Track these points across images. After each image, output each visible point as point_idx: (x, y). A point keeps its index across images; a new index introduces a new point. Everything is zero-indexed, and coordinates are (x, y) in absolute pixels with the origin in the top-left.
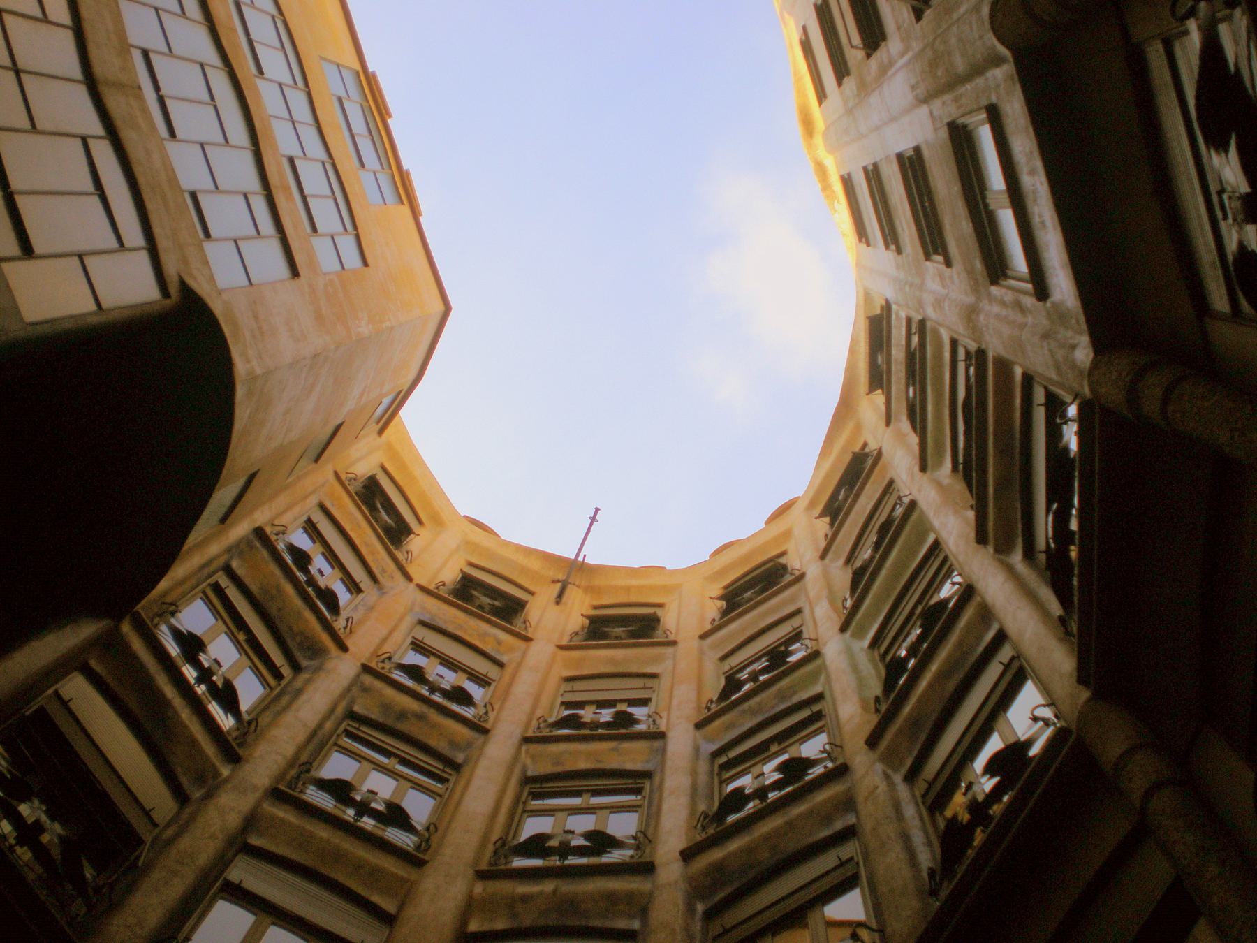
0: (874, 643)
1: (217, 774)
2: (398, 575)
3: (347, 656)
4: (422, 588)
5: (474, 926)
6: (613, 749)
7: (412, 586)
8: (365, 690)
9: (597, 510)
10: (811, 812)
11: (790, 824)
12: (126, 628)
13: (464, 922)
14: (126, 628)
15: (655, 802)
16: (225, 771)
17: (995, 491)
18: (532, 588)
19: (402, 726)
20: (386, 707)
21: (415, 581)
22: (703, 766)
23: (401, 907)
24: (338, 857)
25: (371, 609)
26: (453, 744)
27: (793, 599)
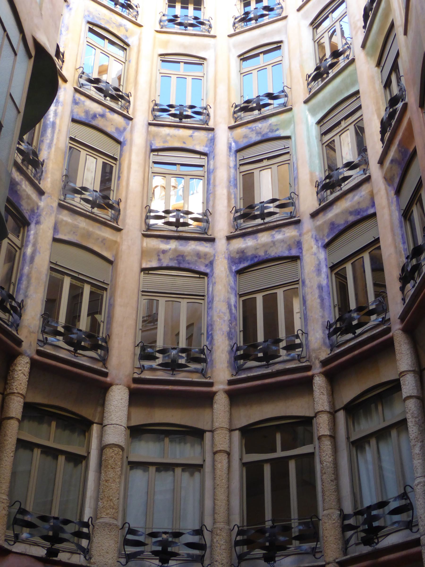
0: (318, 123)
5: (144, 266)
6: (191, 136)
10: (283, 241)
11: (274, 243)
13: (141, 264)
15: (212, 181)
16: (42, 204)
17: (392, 161)
19: (94, 123)
20: (87, 112)
22: (232, 164)
23: (116, 256)
24: (88, 235)
25: (68, 29)
26: (117, 129)
27: (279, 31)
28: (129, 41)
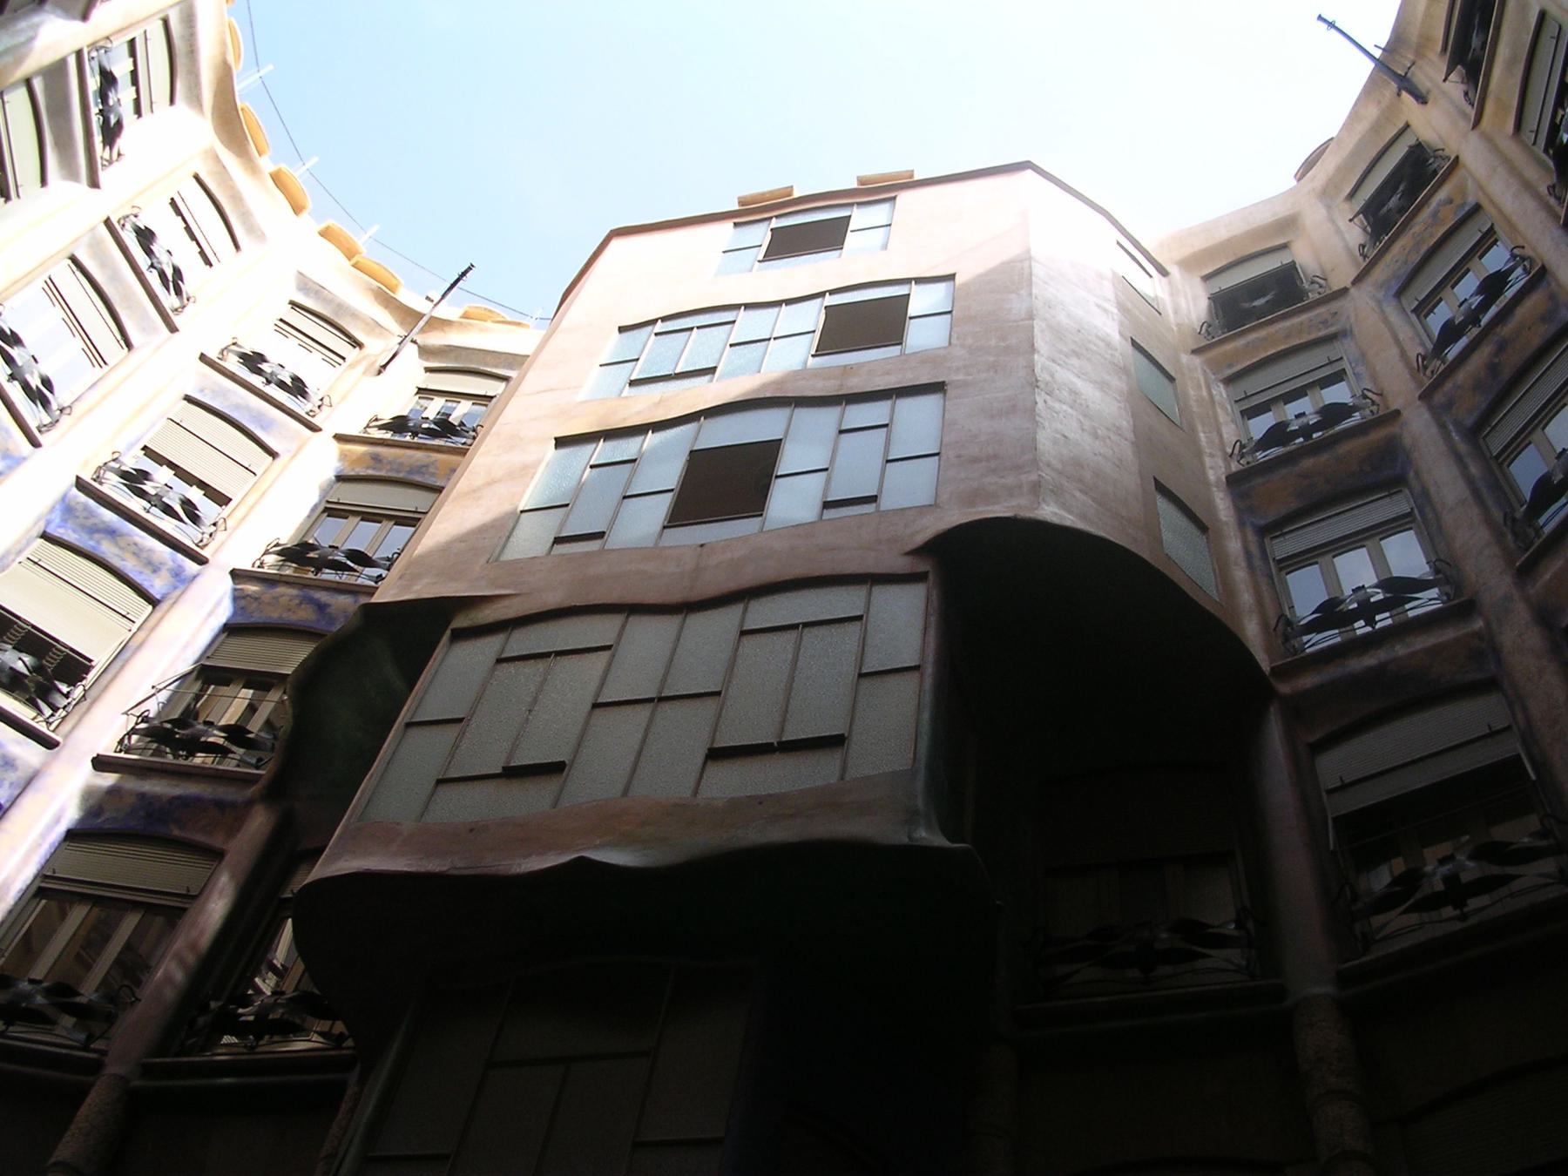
1: (1478, 635)
2: (1335, 306)
3: (1405, 413)
4: (1357, 280)
7: (1353, 291)
8: (1449, 405)
9: (1320, 18)
12: (1284, 688)
14: (1284, 688)
18: (1401, 125)
19: (1506, 373)
20: (1478, 386)
21: (1348, 284)
25: (1363, 355)
26: (1545, 318)
28: (1471, 200)
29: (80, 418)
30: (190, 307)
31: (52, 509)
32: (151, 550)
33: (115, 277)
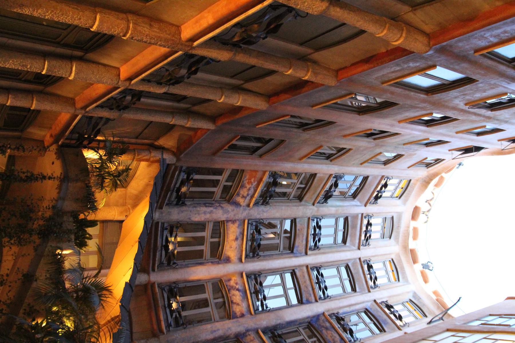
29: (332, 300)
30: (377, 289)
31: (314, 317)
32: (335, 337)
33: (358, 273)
